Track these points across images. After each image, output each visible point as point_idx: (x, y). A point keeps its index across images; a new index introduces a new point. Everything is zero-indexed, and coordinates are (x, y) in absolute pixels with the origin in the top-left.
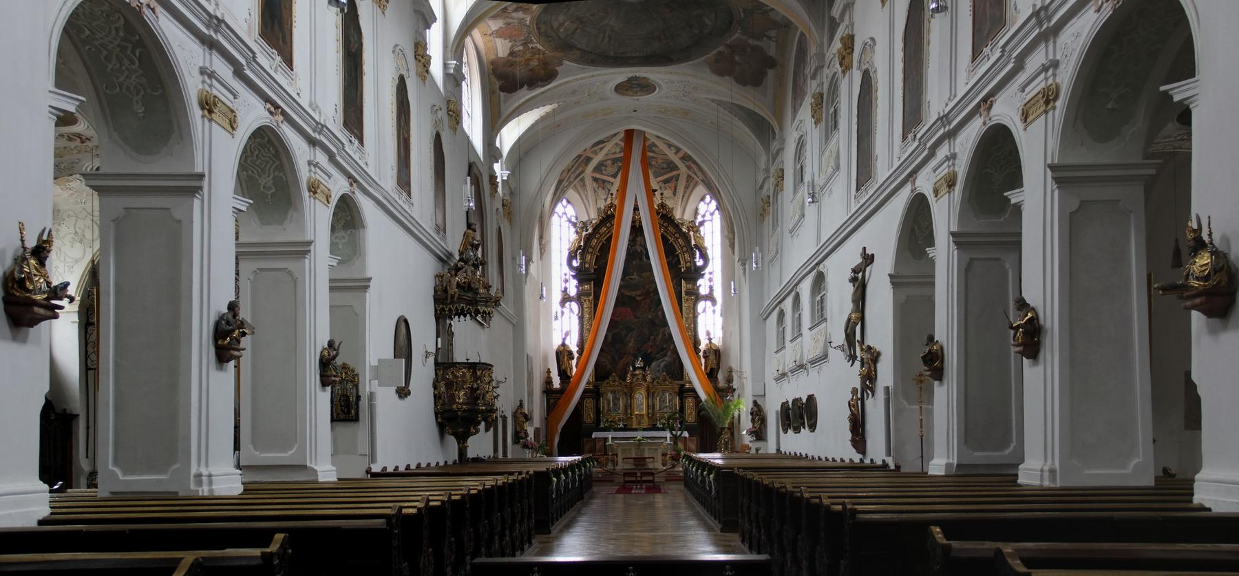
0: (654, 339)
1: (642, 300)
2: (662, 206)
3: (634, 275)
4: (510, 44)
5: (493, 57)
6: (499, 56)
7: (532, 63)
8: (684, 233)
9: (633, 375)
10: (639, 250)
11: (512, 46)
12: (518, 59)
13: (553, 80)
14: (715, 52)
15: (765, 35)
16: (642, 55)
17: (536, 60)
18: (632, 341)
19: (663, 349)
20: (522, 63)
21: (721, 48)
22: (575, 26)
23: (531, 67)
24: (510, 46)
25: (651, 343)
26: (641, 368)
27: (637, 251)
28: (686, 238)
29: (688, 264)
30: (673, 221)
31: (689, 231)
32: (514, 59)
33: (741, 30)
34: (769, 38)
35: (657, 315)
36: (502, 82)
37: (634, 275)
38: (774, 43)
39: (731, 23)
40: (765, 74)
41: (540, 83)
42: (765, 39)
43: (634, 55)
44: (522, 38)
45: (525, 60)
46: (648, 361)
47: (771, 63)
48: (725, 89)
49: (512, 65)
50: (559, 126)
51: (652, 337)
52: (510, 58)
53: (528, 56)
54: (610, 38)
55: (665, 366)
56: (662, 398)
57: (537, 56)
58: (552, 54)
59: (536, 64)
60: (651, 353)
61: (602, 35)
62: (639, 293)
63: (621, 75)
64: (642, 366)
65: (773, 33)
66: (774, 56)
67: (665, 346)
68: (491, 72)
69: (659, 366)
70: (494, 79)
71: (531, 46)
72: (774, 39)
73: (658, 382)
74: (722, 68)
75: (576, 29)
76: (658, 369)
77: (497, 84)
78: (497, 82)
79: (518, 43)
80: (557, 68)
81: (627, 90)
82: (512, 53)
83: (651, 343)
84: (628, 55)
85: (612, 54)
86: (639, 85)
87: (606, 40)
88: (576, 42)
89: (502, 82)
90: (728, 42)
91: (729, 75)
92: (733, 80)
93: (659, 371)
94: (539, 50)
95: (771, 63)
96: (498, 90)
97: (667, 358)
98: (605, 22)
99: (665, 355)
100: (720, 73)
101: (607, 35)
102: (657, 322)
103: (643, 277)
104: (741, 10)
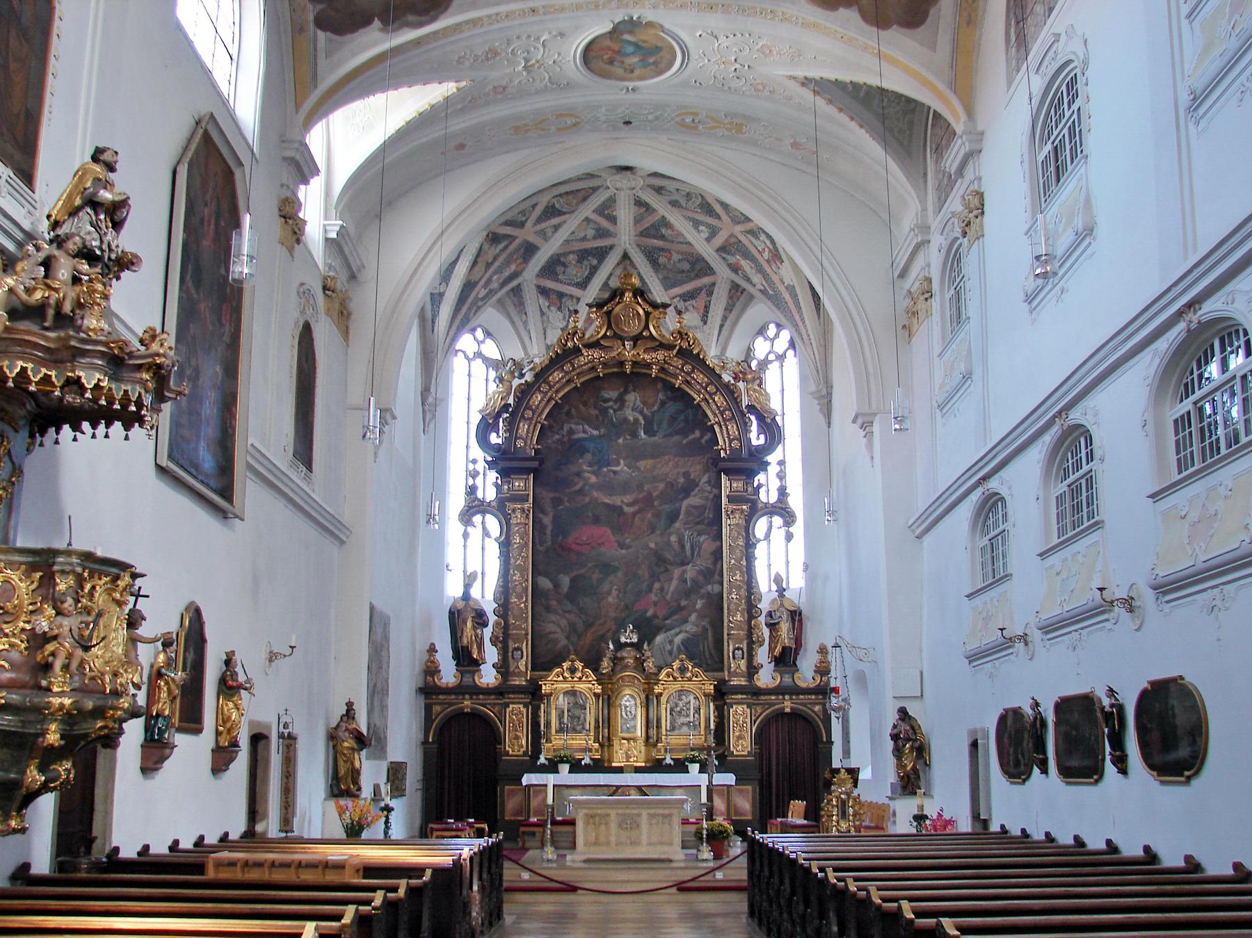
0: (662, 589)
1: (634, 514)
2: (679, 333)
3: (618, 464)
8: (727, 386)
9: (616, 660)
10: (631, 419)
13: (443, 12)
18: (614, 593)
19: (681, 609)
25: (653, 597)
26: (632, 645)
27: (626, 420)
28: (730, 392)
29: (735, 444)
30: (703, 361)
31: (736, 378)
35: (669, 544)
36: (320, 7)
37: (618, 464)
41: (411, 18)
46: (647, 631)
50: (461, 147)
51: (657, 585)
55: (684, 642)
56: (677, 705)
60: (655, 616)
62: (628, 498)
64: (635, 640)
67: (683, 603)
69: (671, 642)
73: (668, 675)
76: (669, 647)
78: (310, 7)
83: (653, 597)
89: (320, 7)
93: (670, 653)
96: (312, 26)
97: (689, 627)
99: (686, 621)
102: (669, 556)
103: (639, 469)
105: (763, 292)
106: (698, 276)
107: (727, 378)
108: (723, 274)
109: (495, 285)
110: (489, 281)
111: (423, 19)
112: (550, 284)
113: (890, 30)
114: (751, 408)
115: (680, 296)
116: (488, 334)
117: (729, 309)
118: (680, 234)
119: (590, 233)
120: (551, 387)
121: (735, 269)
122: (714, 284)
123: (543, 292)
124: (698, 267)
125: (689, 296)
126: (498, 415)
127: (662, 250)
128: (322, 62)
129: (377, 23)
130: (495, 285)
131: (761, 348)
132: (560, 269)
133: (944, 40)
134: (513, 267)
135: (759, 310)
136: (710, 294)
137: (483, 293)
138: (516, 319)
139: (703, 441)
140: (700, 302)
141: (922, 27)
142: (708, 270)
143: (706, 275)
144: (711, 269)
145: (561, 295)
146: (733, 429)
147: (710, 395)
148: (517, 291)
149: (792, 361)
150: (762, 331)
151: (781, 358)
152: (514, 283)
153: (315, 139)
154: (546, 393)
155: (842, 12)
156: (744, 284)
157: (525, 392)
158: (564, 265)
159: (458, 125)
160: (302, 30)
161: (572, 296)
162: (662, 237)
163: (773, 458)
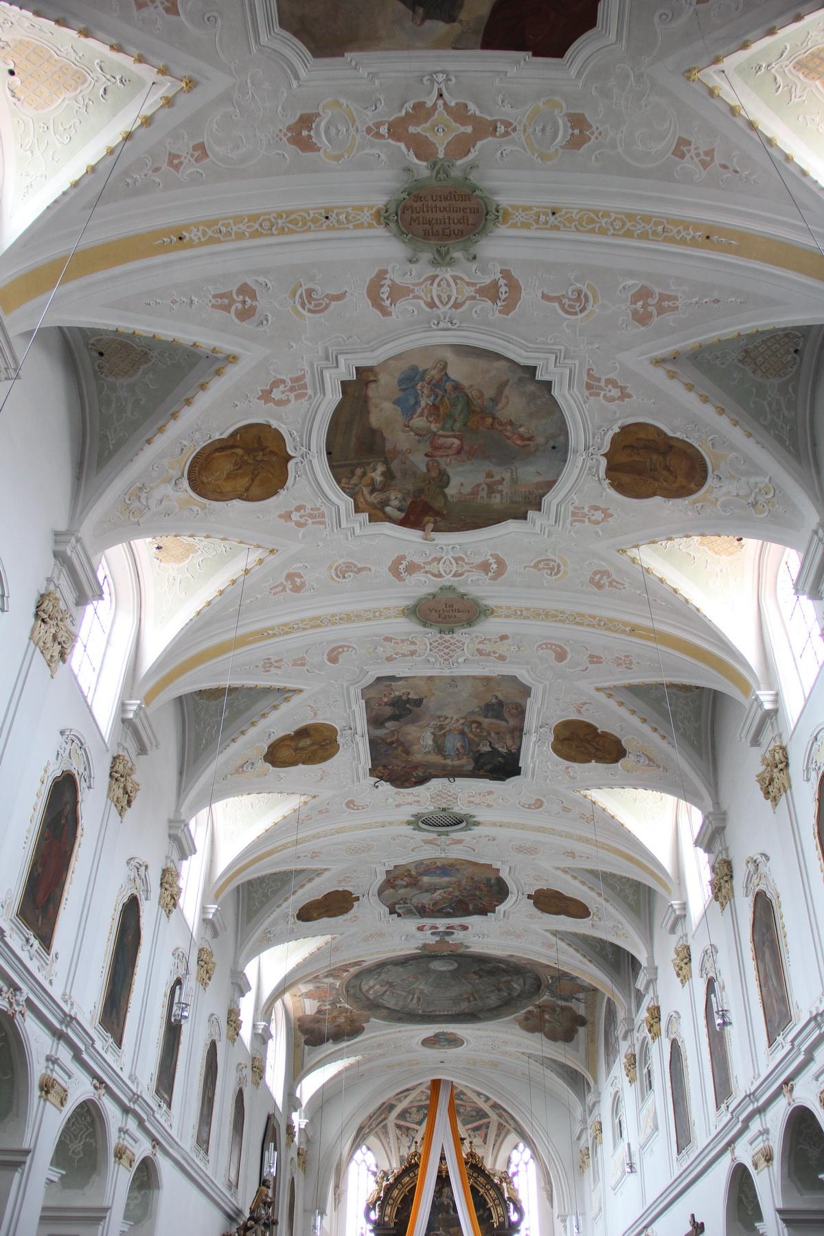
2: (471, 1155)
4: (319, 1004)
5: (301, 1015)
7: (338, 1020)
8: (496, 1185)
10: (446, 1203)
14: (525, 1011)
15: (573, 998)
21: (530, 1008)
22: (385, 989)
23: (337, 1023)
30: (484, 1171)
31: (501, 1181)
32: (322, 1017)
34: (578, 1000)
37: (439, 1230)
39: (539, 987)
40: (576, 1031)
42: (574, 1000)
43: (442, 1013)
44: (331, 998)
47: (582, 1021)
48: (537, 1044)
49: (319, 1021)
50: (362, 1075)
53: (335, 1013)
54: (419, 999)
57: (344, 1014)
58: (359, 1012)
61: (411, 997)
63: (430, 1030)
65: (581, 996)
70: (299, 1034)
71: (338, 1005)
74: (533, 1024)
75: (386, 992)
80: (364, 1025)
81: (434, 1044)
82: (319, 1011)
84: (437, 1013)
85: (420, 1012)
86: (446, 1040)
87: (415, 1001)
90: (537, 1003)
91: (540, 1031)
92: (543, 1036)
95: (582, 1021)
98: (415, 986)
100: (531, 1029)
101: (416, 996)
105: (515, 1129)
106: (480, 1119)
107: (496, 1181)
108: (493, 1117)
109: (374, 1126)
110: (371, 1124)
112: (402, 1123)
114: (509, 1199)
115: (471, 1129)
116: (369, 1149)
117: (498, 1135)
118: (470, 1098)
119: (424, 1098)
120: (403, 1186)
121: (500, 1116)
122: (489, 1123)
123: (399, 1127)
124: (481, 1114)
125: (476, 1129)
126: (376, 1202)
127: (461, 1105)
129: (331, 1041)
130: (374, 1126)
131: (515, 1156)
132: (408, 1115)
133: (582, 1048)
134: (383, 1116)
135: (513, 1138)
136: (488, 1128)
137: (367, 1131)
138: (382, 1137)
139: (485, 1216)
140: (482, 1132)
142: (486, 1115)
143: (485, 1118)
144: (487, 1114)
145: (408, 1129)
146: (500, 1210)
147: (488, 1190)
148: (385, 1127)
149: (532, 1165)
150: (516, 1147)
151: (526, 1164)
152: (384, 1123)
153: (250, 971)
154: (400, 1190)
156: (505, 1124)
157: (389, 1189)
158: (410, 1113)
159: (362, 1068)
160: (298, 1046)
161: (413, 1129)
162: (462, 1100)
163: (522, 1227)
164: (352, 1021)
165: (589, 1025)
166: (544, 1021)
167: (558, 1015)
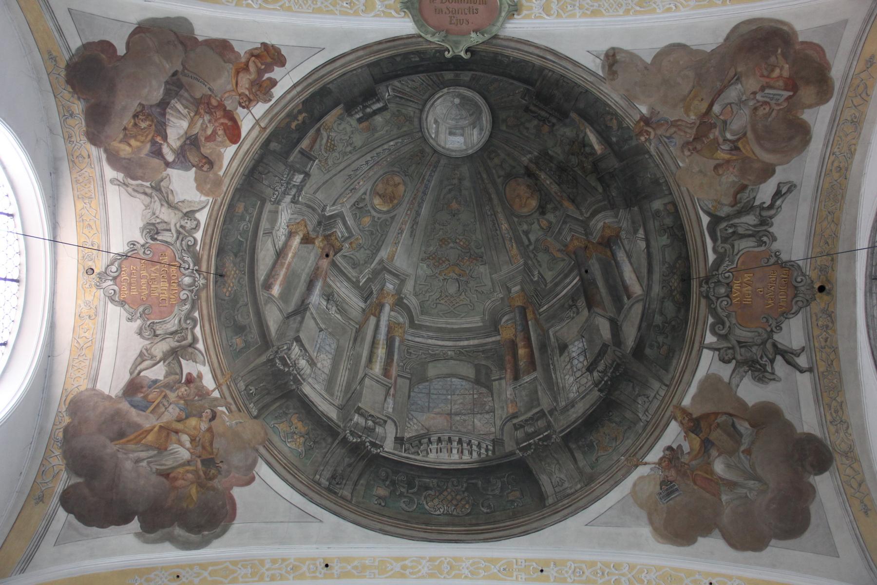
5: (83, 385)
6: (99, 386)
11: (141, 357)
12: (147, 420)
13: (218, 536)
16: (466, 457)
17: (185, 438)
20: (150, 438)
24: (134, 354)
33: (714, 332)
38: (807, 374)
41: (178, 531)
44: (172, 324)
45: (161, 427)
49: (121, 435)
52: (125, 406)
57: (193, 422)
59: (185, 455)
66: (817, 432)
68: (61, 435)
72: (802, 361)
77: (63, 481)
78: (64, 475)
79: (161, 348)
88: (303, 363)
94: (203, 393)
96: (56, 500)
104: (705, 220)
111: (193, 537)
113: (769, 548)
128: (47, 548)
133: (843, 538)
141: (807, 534)
155: (703, 542)
160: (41, 499)
164: (209, 462)
165: (838, 459)
166: (713, 483)
167: (748, 452)
